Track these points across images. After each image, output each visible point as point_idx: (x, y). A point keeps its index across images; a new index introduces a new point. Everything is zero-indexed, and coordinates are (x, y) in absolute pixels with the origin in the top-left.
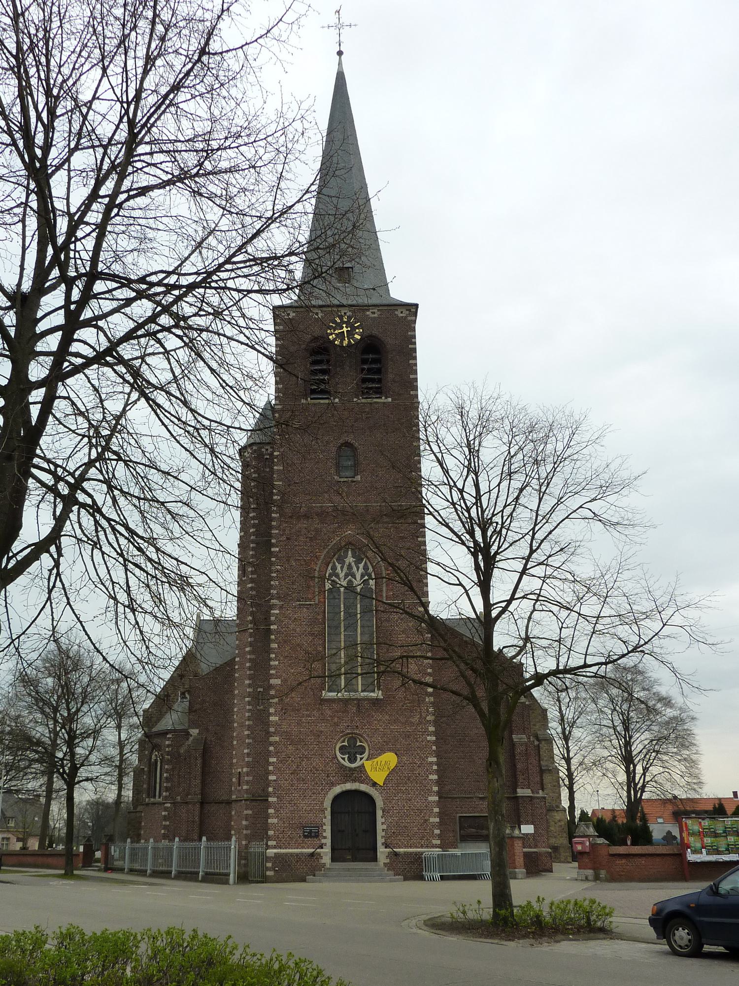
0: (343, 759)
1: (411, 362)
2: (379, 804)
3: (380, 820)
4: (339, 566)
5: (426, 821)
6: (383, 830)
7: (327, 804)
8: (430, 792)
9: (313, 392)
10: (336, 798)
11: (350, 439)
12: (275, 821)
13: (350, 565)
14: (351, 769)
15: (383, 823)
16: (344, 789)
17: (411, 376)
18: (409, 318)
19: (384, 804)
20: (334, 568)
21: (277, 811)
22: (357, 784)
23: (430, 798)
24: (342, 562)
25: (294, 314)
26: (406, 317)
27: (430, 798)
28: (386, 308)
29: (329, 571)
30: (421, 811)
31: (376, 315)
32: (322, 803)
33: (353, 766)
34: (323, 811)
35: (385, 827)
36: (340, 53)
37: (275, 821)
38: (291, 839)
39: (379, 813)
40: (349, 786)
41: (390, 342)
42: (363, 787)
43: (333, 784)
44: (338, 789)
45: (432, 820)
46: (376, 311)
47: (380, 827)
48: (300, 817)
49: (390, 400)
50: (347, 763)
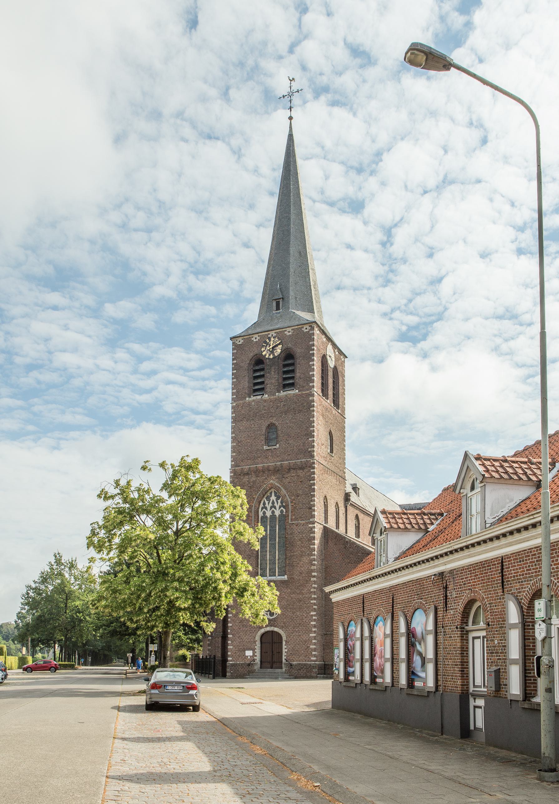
1: (311, 363)
2: (284, 638)
3: (284, 647)
4: (267, 502)
5: (308, 647)
6: (286, 652)
7: (258, 638)
8: (311, 632)
9: (255, 391)
10: (262, 636)
11: (273, 421)
12: (231, 647)
13: (273, 503)
15: (285, 649)
16: (266, 630)
17: (311, 373)
18: (311, 332)
19: (287, 638)
20: (264, 504)
22: (273, 628)
23: (311, 635)
24: (269, 500)
25: (243, 341)
26: (309, 331)
27: (311, 635)
28: (296, 327)
29: (262, 505)
30: (306, 642)
31: (290, 333)
32: (255, 638)
33: (271, 618)
34: (255, 642)
35: (286, 650)
36: (291, 118)
37: (231, 647)
39: (284, 643)
41: (298, 351)
42: (276, 629)
45: (311, 647)
47: (284, 650)
48: (244, 645)
49: (297, 391)
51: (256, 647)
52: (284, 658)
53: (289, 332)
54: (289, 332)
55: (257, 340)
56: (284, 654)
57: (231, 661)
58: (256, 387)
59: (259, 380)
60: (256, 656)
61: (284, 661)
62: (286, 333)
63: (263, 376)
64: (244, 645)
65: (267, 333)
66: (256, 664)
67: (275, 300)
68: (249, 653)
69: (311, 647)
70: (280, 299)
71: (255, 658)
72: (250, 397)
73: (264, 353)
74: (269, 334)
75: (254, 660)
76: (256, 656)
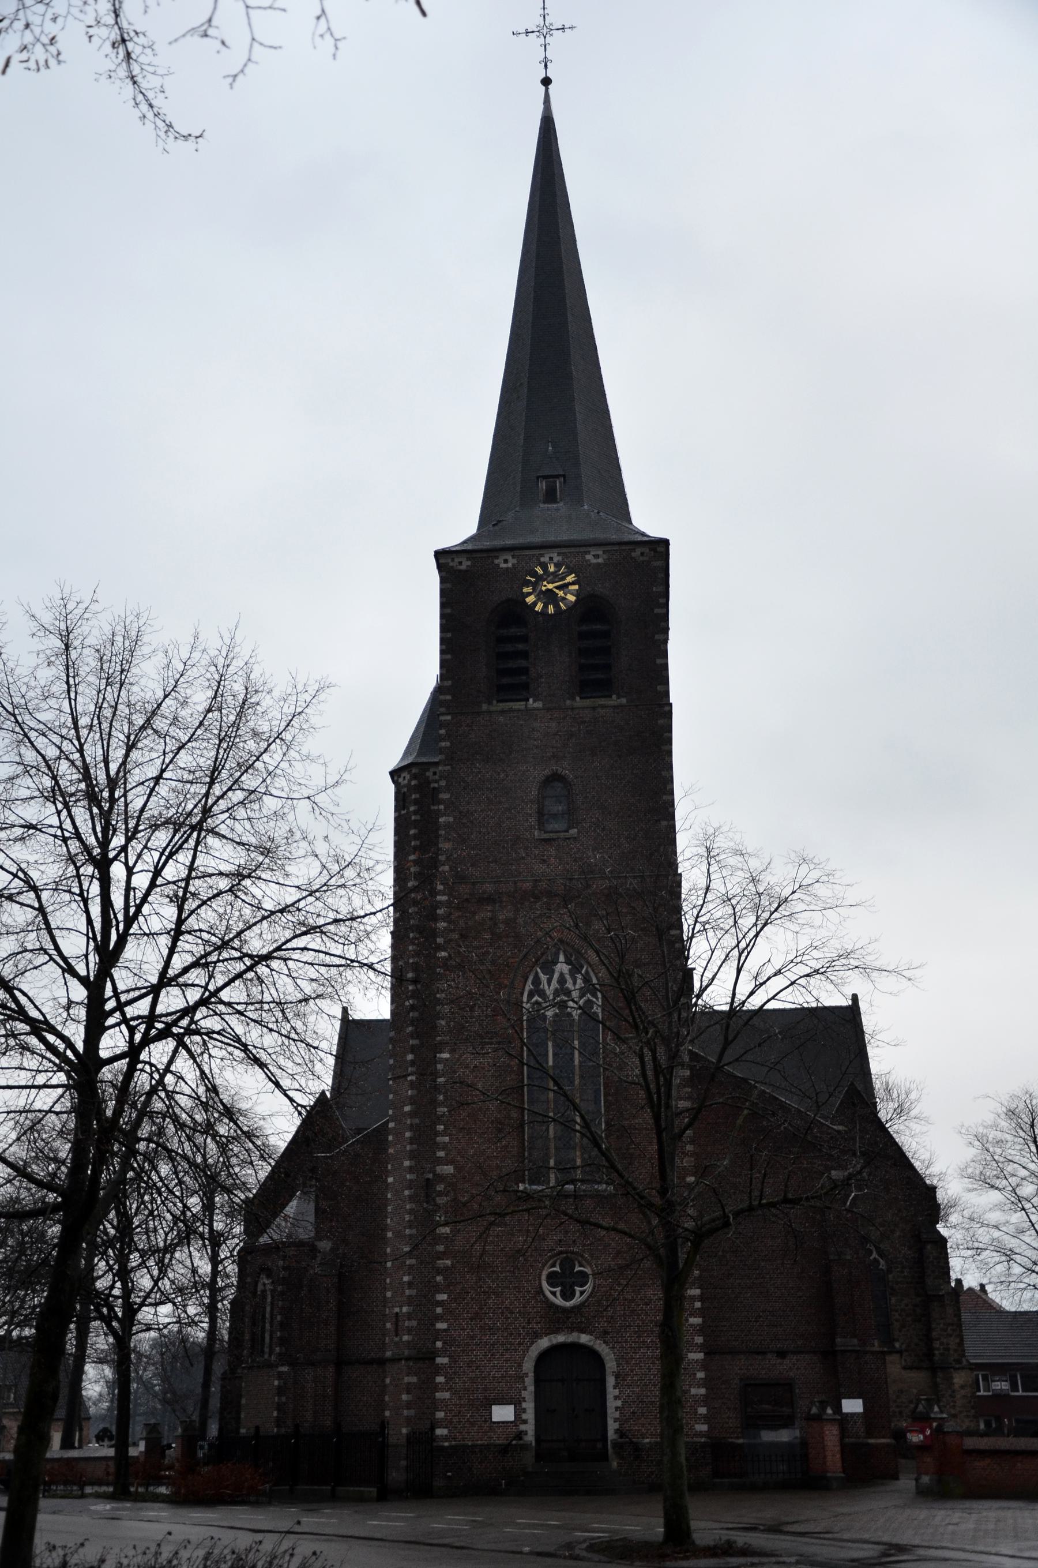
0: (554, 1294)
1: (657, 637)
3: (611, 1391)
4: (543, 978)
6: (617, 1408)
7: (528, 1366)
10: (543, 1357)
12: (447, 1395)
13: (562, 980)
14: (564, 1310)
15: (616, 1398)
16: (554, 1342)
19: (618, 1365)
20: (537, 981)
21: (448, 1379)
22: (575, 1334)
24: (550, 973)
25: (469, 563)
28: (616, 548)
29: (529, 986)
31: (600, 560)
32: (520, 1366)
33: (568, 1304)
34: (521, 1378)
35: (619, 1403)
36: (546, 82)
37: (447, 1395)
38: (473, 1424)
39: (611, 1381)
40: (561, 1338)
42: (584, 1339)
43: (536, 1336)
44: (544, 1343)
45: (693, 1391)
46: (600, 553)
48: (485, 1389)
50: (559, 1301)
51: (524, 1394)
52: (612, 1426)
53: (597, 556)
54: (597, 556)
55: (510, 565)
56: (612, 1414)
57: (446, 1438)
58: (505, 681)
59: (512, 664)
60: (525, 1422)
61: (611, 1434)
62: (588, 557)
63: (525, 655)
64: (485, 1389)
65: (537, 552)
66: (525, 1447)
67: (545, 477)
68: (502, 1413)
69: (693, 1391)
70: (557, 476)
71: (523, 1427)
72: (490, 703)
73: (530, 600)
74: (542, 555)
75: (520, 1435)
76: (525, 1422)
